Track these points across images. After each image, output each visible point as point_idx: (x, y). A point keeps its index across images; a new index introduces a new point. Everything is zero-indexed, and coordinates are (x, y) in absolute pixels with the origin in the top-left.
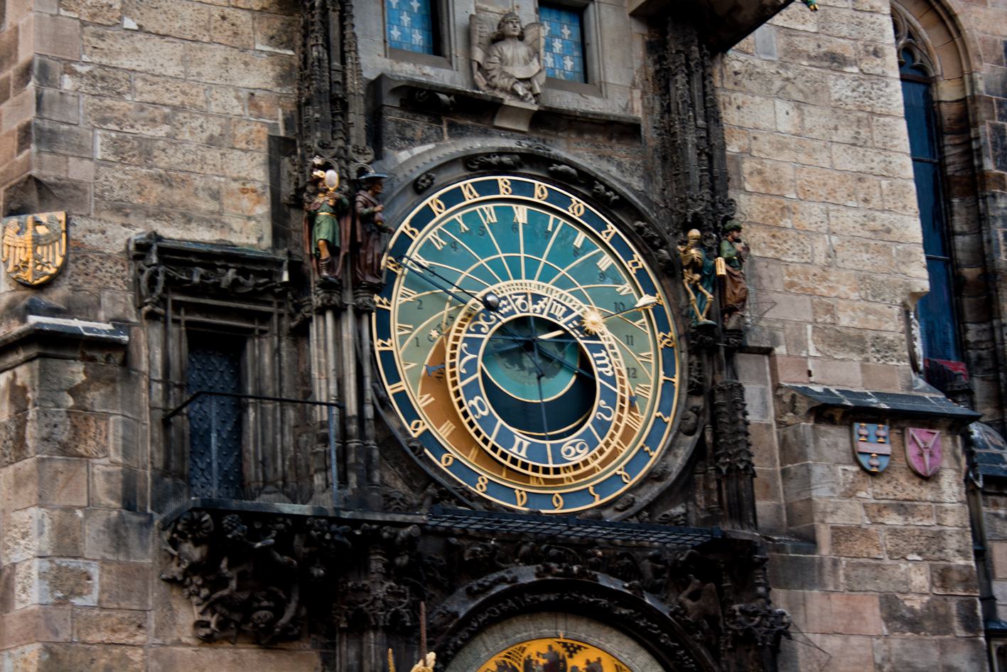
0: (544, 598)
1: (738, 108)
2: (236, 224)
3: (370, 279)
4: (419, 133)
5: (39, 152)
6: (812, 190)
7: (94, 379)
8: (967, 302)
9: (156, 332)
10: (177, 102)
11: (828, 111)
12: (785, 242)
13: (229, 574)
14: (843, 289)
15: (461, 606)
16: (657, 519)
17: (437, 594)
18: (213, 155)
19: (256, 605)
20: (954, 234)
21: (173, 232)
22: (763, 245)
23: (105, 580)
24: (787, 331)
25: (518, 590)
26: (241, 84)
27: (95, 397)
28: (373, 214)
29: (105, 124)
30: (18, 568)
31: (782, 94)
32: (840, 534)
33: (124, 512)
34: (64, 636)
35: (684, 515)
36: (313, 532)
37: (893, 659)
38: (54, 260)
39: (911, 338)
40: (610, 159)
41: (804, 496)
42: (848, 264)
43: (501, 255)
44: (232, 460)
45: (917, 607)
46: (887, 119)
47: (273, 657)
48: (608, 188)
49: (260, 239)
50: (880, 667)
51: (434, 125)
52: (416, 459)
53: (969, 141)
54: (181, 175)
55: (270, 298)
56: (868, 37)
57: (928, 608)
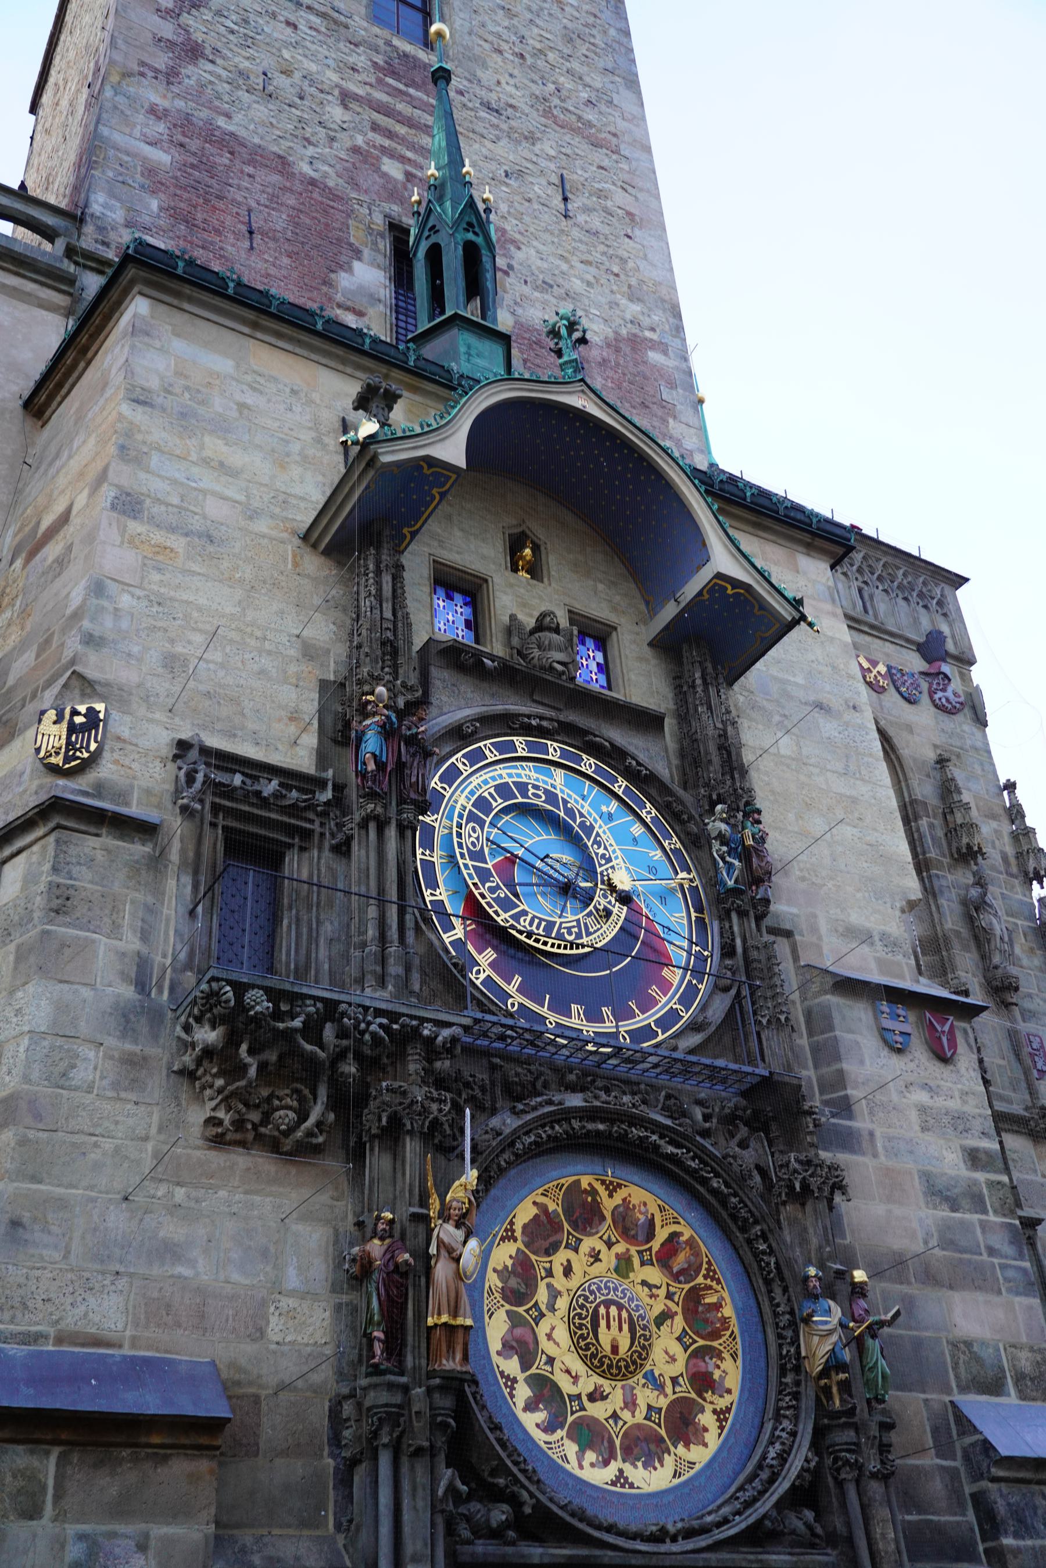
0: (590, 1126)
3: (413, 795)
13: (249, 1060)
15: (506, 1122)
21: (214, 742)
25: (566, 1115)
36: (345, 1020)
47: (293, 1171)
48: (639, 764)
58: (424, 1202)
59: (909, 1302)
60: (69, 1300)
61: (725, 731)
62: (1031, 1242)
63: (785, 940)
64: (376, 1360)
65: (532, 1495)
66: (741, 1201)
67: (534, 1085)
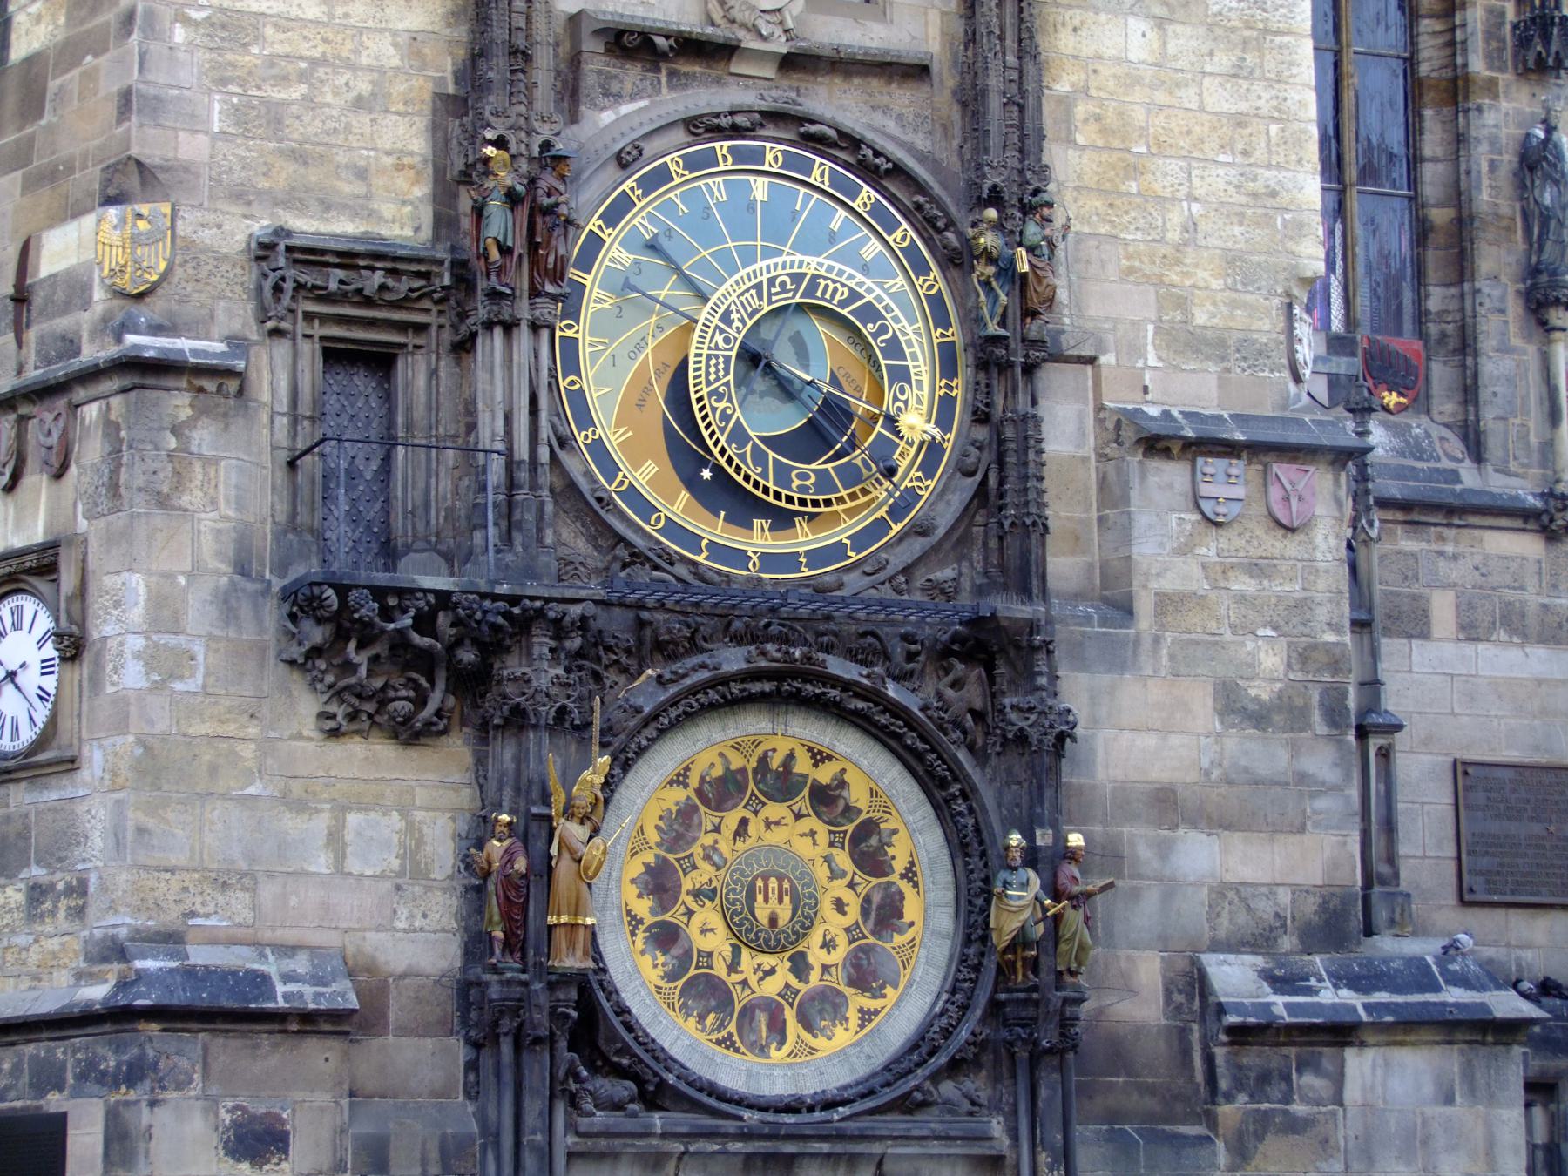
0: (756, 687)
1: (1075, 30)
2: (388, 209)
3: (550, 288)
4: (628, 87)
5: (141, 126)
6: (1170, 141)
7: (200, 412)
8: (1432, 256)
9: (282, 348)
10: (316, 53)
11: (1201, 30)
12: (1127, 212)
13: (356, 659)
14: (1202, 275)
16: (918, 584)
17: (622, 679)
18: (361, 122)
19: (392, 694)
20: (1422, 160)
21: (307, 226)
22: (1095, 218)
23: (211, 660)
25: (725, 681)
26: (400, 26)
27: (203, 437)
28: (557, 205)
29: (225, 85)
30: (110, 643)
32: (1167, 604)
33: (237, 577)
34: (160, 727)
37: (1225, 763)
38: (157, 263)
39: (1291, 338)
40: (886, 110)
41: (1122, 553)
42: (1212, 242)
43: (731, 244)
44: (378, 505)
45: (1265, 696)
46: (1286, 39)
47: (414, 753)
48: (877, 154)
49: (417, 230)
50: (1207, 773)
51: (650, 75)
53: (1453, 30)
54: (319, 149)
55: (426, 304)
57: (1280, 698)
58: (546, 799)
59: (1164, 849)
60: (198, 900)
61: (1021, 72)
62: (1385, 754)
63: (1089, 368)
64: (494, 961)
65: (656, 1074)
67: (691, 639)
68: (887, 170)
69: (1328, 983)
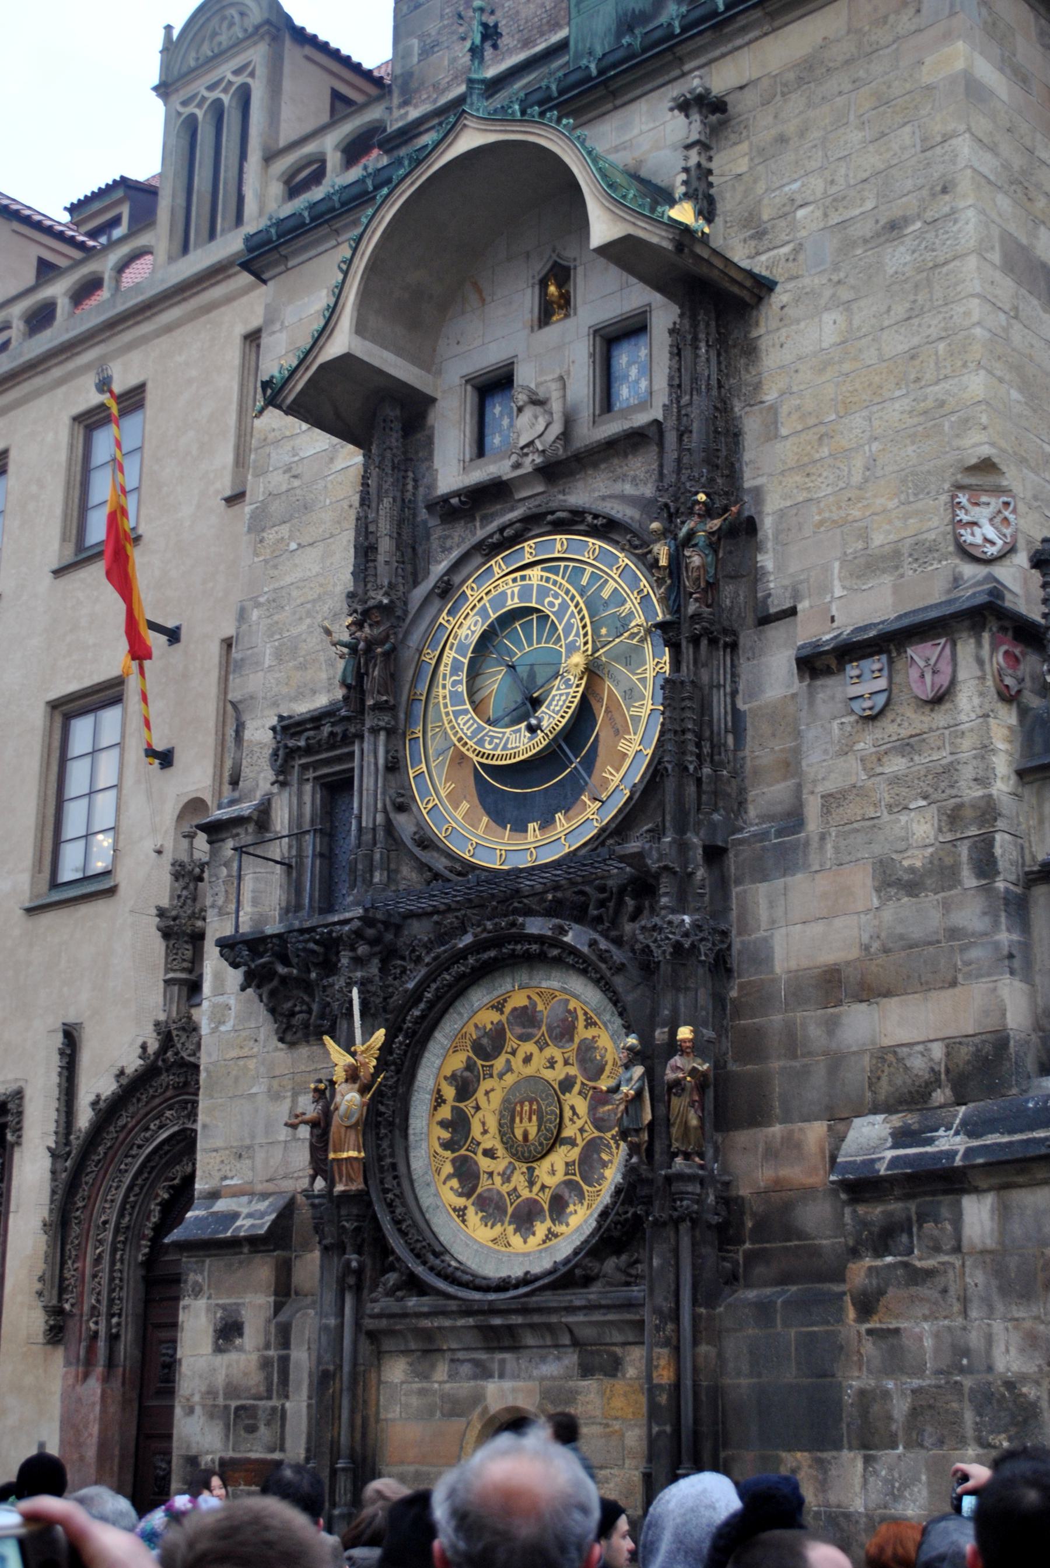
0: (485, 956)
4: (456, 539)
12: (820, 475)
24: (812, 580)
25: (462, 955)
31: (835, 303)
34: (214, 1058)
35: (649, 831)
37: (883, 935)
40: (623, 478)
45: (918, 864)
46: (951, 266)
48: (596, 516)
50: (867, 948)
52: (417, 851)
54: (313, 656)
56: (936, 175)
57: (931, 862)
61: (690, 404)
66: (607, 983)
68: (602, 525)
69: (952, 1132)
